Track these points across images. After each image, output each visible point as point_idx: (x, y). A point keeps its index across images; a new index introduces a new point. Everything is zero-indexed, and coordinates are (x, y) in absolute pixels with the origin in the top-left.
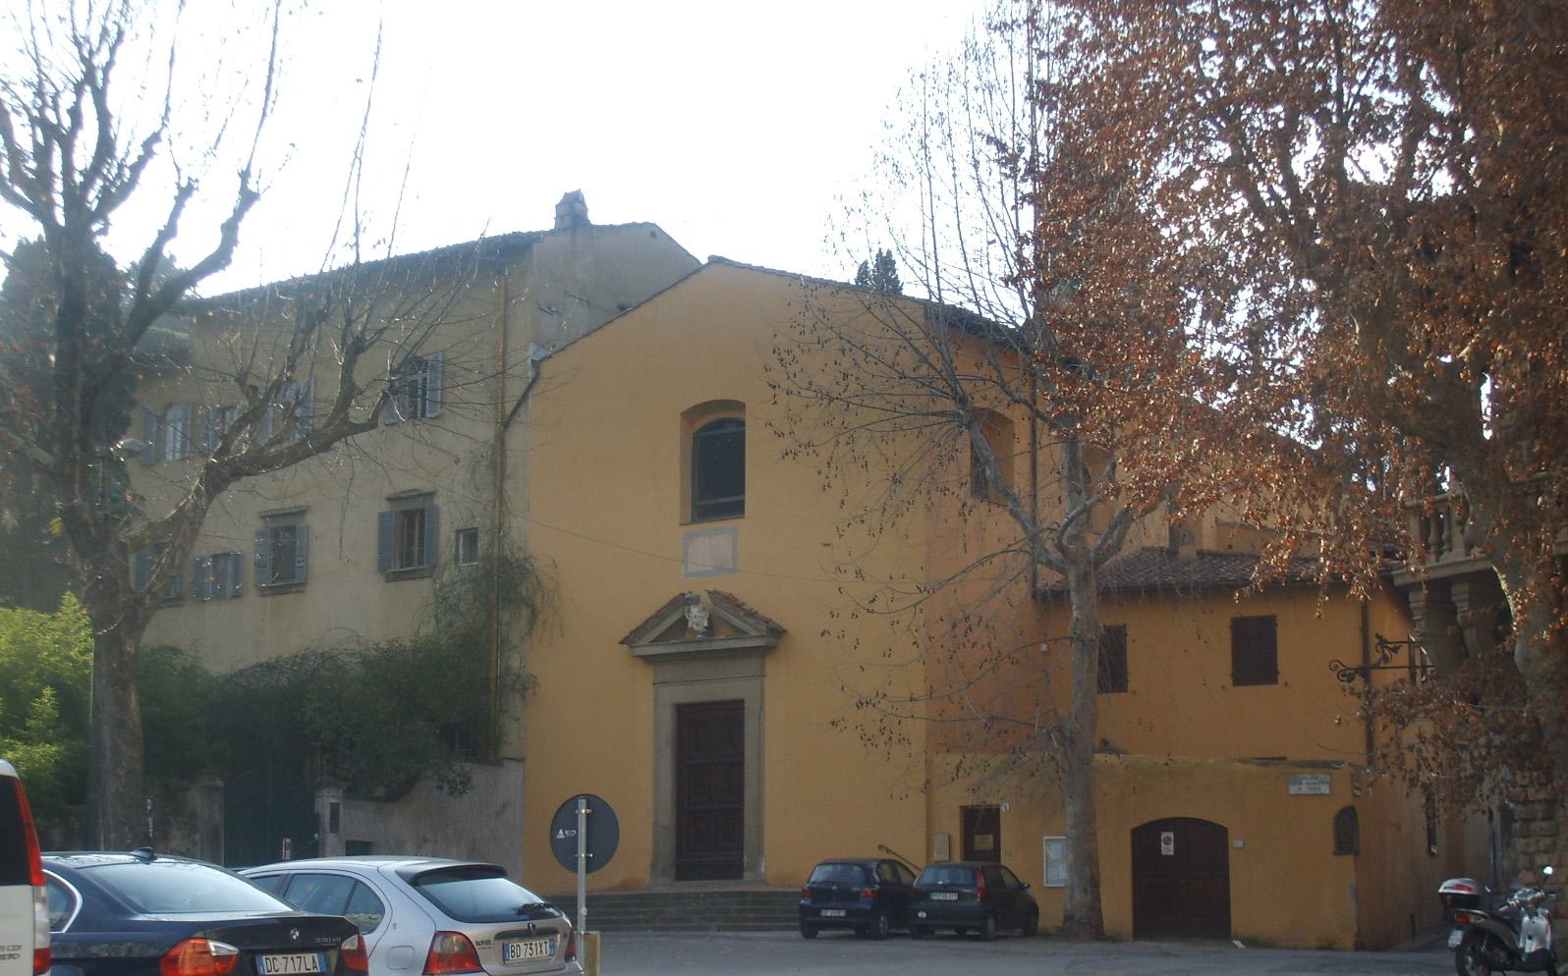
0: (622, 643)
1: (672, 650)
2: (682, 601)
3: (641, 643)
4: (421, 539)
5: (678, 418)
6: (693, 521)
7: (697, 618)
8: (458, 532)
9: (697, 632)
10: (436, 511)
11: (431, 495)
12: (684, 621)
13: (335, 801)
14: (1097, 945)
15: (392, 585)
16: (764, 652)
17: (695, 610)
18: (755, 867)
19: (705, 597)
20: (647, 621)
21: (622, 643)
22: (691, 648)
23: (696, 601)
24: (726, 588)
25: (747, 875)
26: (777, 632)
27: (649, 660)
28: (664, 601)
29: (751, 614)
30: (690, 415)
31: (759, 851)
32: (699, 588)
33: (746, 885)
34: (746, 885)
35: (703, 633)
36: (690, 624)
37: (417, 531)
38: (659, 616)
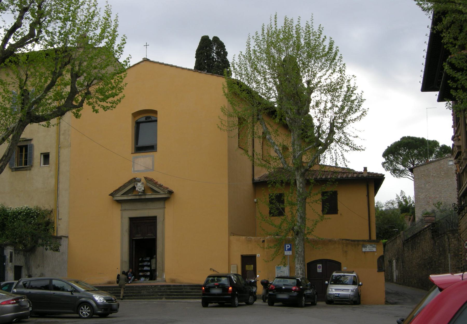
0: (110, 195)
1: (130, 198)
2: (135, 180)
3: (117, 195)
4: (26, 155)
5: (131, 115)
6: (135, 153)
7: (140, 187)
8: (41, 154)
9: (139, 192)
10: (32, 146)
11: (31, 140)
12: (134, 188)
13: (11, 251)
14: (248, 306)
15: (14, 172)
16: (165, 200)
17: (139, 184)
18: (162, 276)
19: (143, 180)
20: (120, 187)
21: (110, 195)
22: (138, 197)
23: (139, 181)
24: (150, 176)
25: (158, 279)
26: (171, 192)
27: (119, 202)
28: (127, 181)
29: (161, 186)
30: (135, 115)
31: (163, 270)
32: (141, 176)
33: (158, 282)
34: (158, 282)
35: (142, 192)
36: (137, 189)
37: (24, 153)
38: (125, 186)
